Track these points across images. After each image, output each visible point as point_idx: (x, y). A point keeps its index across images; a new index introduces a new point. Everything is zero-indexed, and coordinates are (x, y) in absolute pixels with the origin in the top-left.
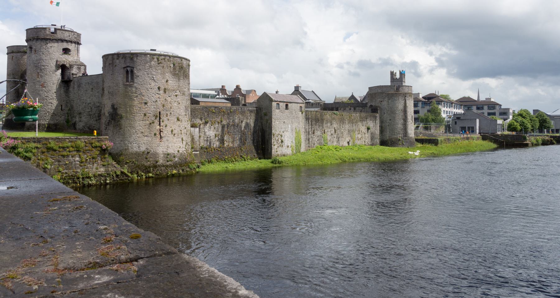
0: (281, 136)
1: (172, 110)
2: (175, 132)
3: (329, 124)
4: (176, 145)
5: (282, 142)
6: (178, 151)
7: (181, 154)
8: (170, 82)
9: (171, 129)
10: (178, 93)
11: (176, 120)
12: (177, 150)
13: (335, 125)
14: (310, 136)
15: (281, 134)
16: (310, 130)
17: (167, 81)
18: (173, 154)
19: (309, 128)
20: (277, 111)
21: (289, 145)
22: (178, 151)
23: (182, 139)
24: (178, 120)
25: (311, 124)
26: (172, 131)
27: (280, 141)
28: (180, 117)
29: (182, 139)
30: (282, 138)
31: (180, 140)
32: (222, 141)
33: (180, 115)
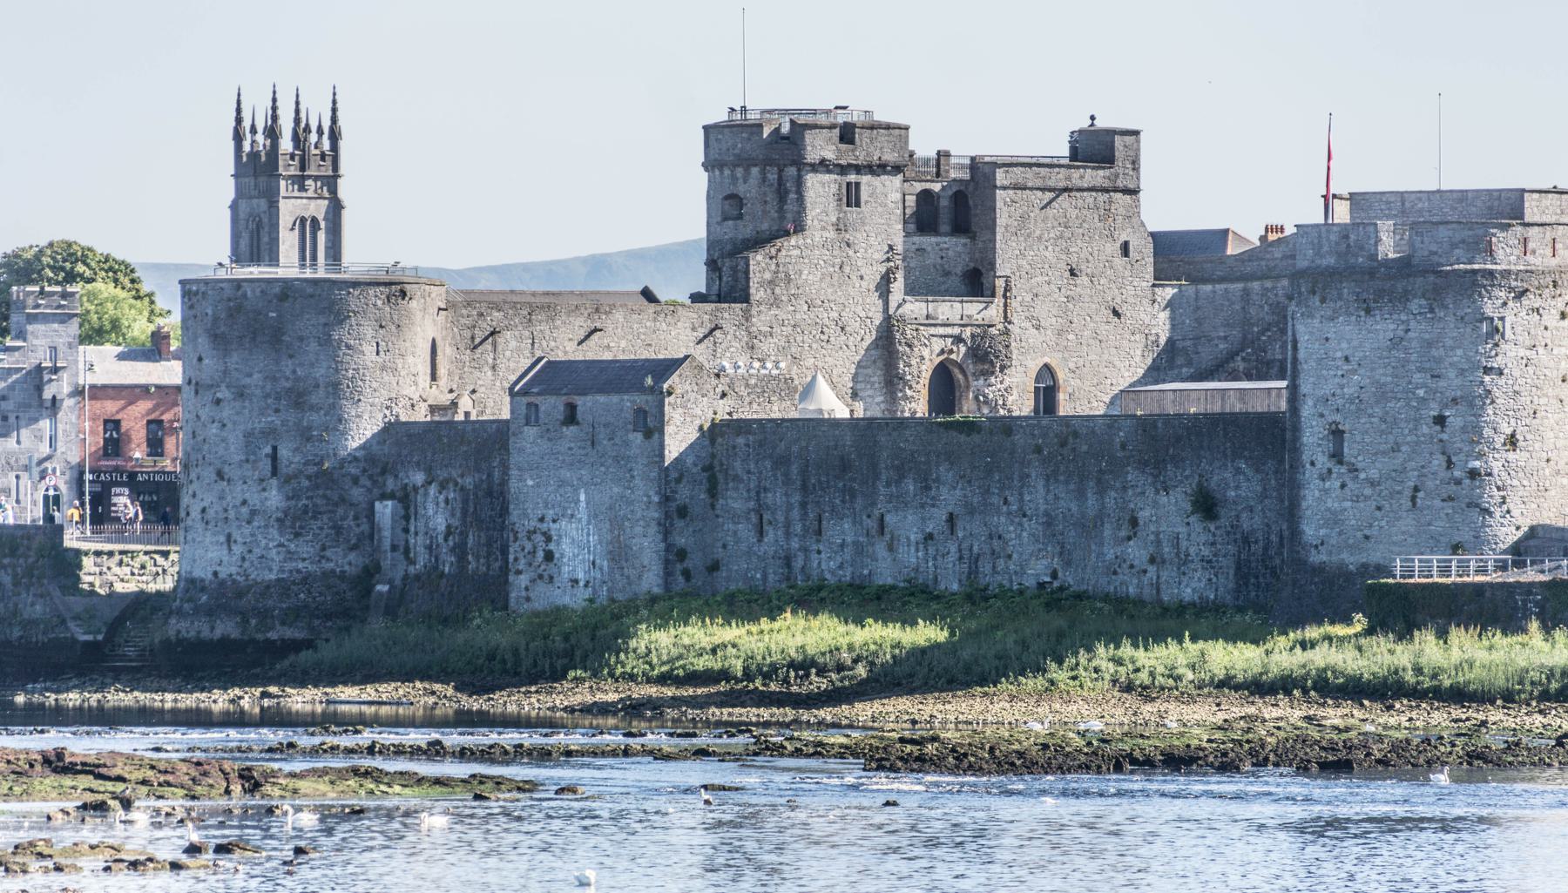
0: (549, 539)
1: (206, 447)
2: (211, 513)
3: (910, 486)
4: (210, 555)
5: (549, 556)
6: (215, 574)
7: (222, 583)
8: (206, 361)
9: (202, 504)
10: (223, 393)
11: (214, 477)
12: (210, 570)
13: (950, 497)
14: (795, 544)
15: (544, 527)
16: (796, 514)
17: (200, 359)
18: (202, 580)
19: (790, 507)
20: (531, 432)
21: (581, 576)
22: (215, 574)
23: (229, 536)
24: (220, 475)
25: (804, 488)
26: (204, 510)
27: (540, 554)
28: (226, 469)
29: (229, 536)
30: (552, 546)
31: (222, 539)
32: (460, 551)
33: (225, 462)
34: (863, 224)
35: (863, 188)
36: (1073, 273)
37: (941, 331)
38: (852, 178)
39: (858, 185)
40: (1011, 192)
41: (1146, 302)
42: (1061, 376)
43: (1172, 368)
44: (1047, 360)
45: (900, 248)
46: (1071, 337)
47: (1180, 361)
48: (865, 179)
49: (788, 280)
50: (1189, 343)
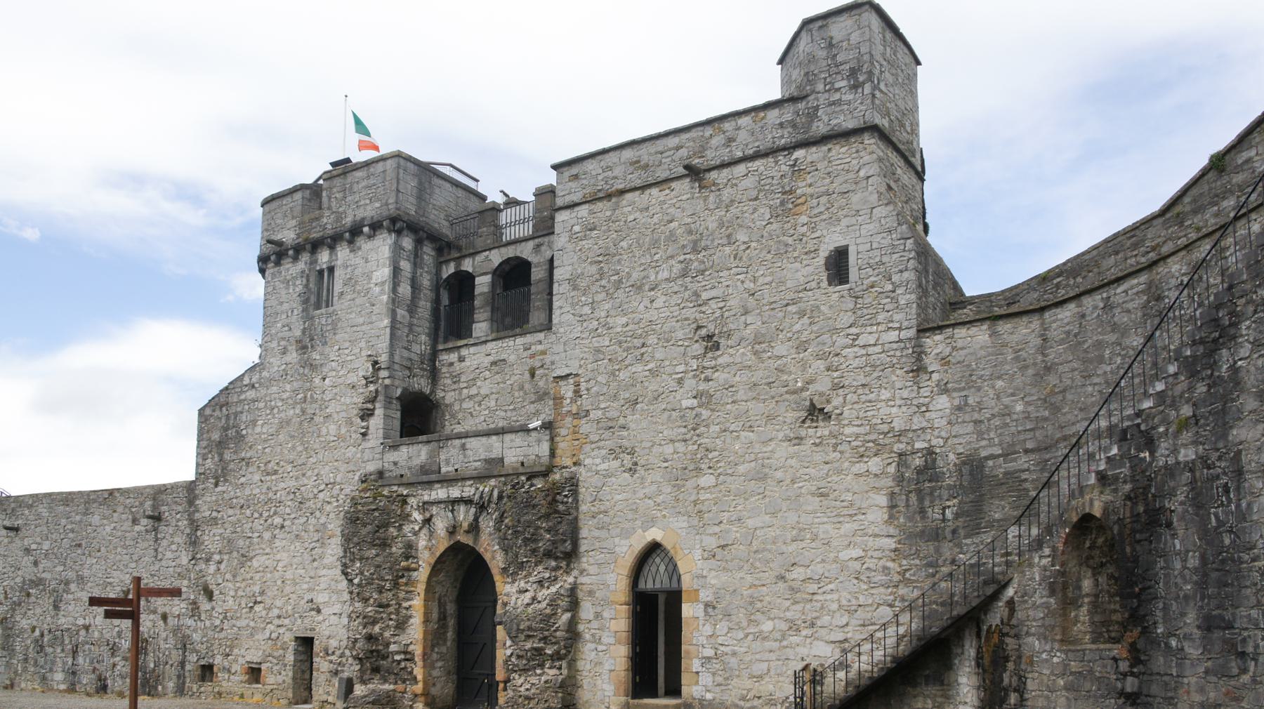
34: (334, 324)
35: (337, 273)
36: (712, 343)
37: (440, 493)
38: (324, 257)
39: (331, 270)
40: (583, 211)
41: (899, 378)
42: (693, 567)
43: (974, 530)
44: (655, 534)
45: (383, 359)
46: (707, 480)
47: (999, 510)
48: (343, 252)
49: (240, 437)
50: (1023, 462)
